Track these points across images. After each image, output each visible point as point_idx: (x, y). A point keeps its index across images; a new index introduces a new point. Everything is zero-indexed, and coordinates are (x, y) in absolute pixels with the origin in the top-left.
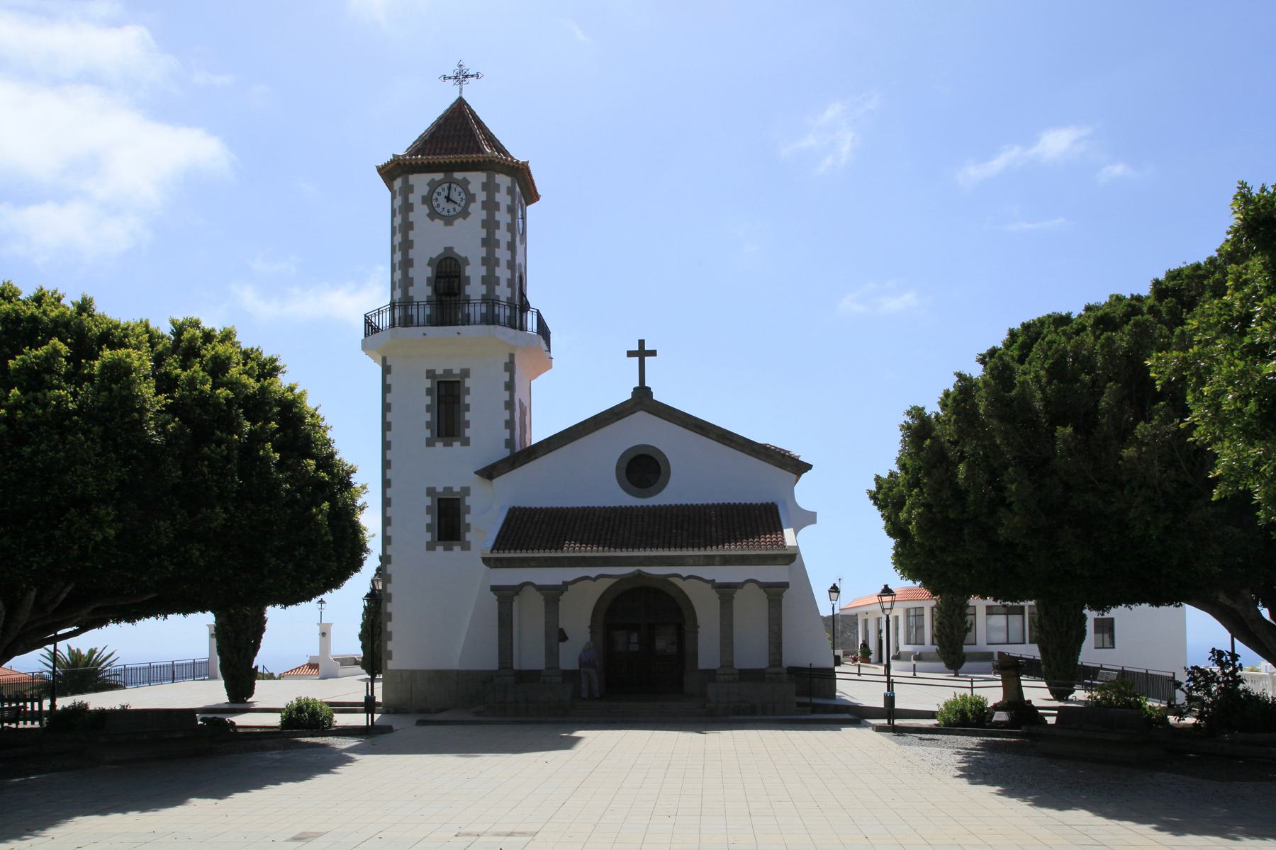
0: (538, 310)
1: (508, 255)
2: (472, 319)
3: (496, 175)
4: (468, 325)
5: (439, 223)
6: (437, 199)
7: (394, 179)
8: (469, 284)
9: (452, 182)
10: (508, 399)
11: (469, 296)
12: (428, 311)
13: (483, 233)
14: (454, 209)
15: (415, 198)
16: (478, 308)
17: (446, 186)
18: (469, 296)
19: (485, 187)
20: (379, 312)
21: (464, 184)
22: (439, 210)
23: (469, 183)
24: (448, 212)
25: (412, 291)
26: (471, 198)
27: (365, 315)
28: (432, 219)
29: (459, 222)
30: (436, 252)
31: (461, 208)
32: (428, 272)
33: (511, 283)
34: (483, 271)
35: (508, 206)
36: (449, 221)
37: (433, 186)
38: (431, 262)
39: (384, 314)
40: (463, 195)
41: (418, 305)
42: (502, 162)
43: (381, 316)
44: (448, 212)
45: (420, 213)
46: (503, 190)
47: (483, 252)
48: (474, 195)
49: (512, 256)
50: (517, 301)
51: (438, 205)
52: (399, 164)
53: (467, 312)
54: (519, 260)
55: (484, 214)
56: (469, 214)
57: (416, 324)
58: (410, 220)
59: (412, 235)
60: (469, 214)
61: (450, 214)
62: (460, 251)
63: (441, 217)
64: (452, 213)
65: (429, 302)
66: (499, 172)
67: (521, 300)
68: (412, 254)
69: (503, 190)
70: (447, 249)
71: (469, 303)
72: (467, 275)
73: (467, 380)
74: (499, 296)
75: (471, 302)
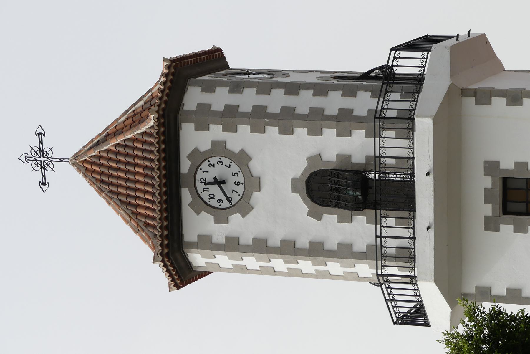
0: (392, 49)
1: (307, 95)
2: (405, 153)
3: (185, 108)
4: (414, 158)
6: (219, 201)
7: (188, 265)
11: (368, 158)
12: (392, 222)
13: (273, 131)
14: (234, 175)
16: (389, 143)
17: (200, 187)
18: (368, 158)
19: (202, 127)
20: (393, 300)
23: (196, 150)
24: (238, 184)
25: (361, 246)
27: (395, 323)
29: (256, 167)
31: (233, 165)
33: (350, 92)
34: (330, 133)
39: (395, 292)
40: (214, 160)
41: (381, 237)
42: (165, 98)
43: (397, 297)
44: (238, 184)
46: (206, 98)
47: (301, 132)
48: (214, 143)
49: (308, 88)
52: (167, 255)
53: (393, 161)
54: (312, 79)
55: (244, 129)
56: (242, 151)
57: (411, 241)
58: (250, 242)
59: (275, 241)
60: (242, 151)
61: (242, 181)
63: (246, 196)
64: (240, 178)
65: (377, 221)
67: (267, 74)
69: (206, 98)
70: (294, 191)
71: (380, 157)
72: (335, 159)
73: (503, 166)
74: (369, 110)
75: (377, 154)
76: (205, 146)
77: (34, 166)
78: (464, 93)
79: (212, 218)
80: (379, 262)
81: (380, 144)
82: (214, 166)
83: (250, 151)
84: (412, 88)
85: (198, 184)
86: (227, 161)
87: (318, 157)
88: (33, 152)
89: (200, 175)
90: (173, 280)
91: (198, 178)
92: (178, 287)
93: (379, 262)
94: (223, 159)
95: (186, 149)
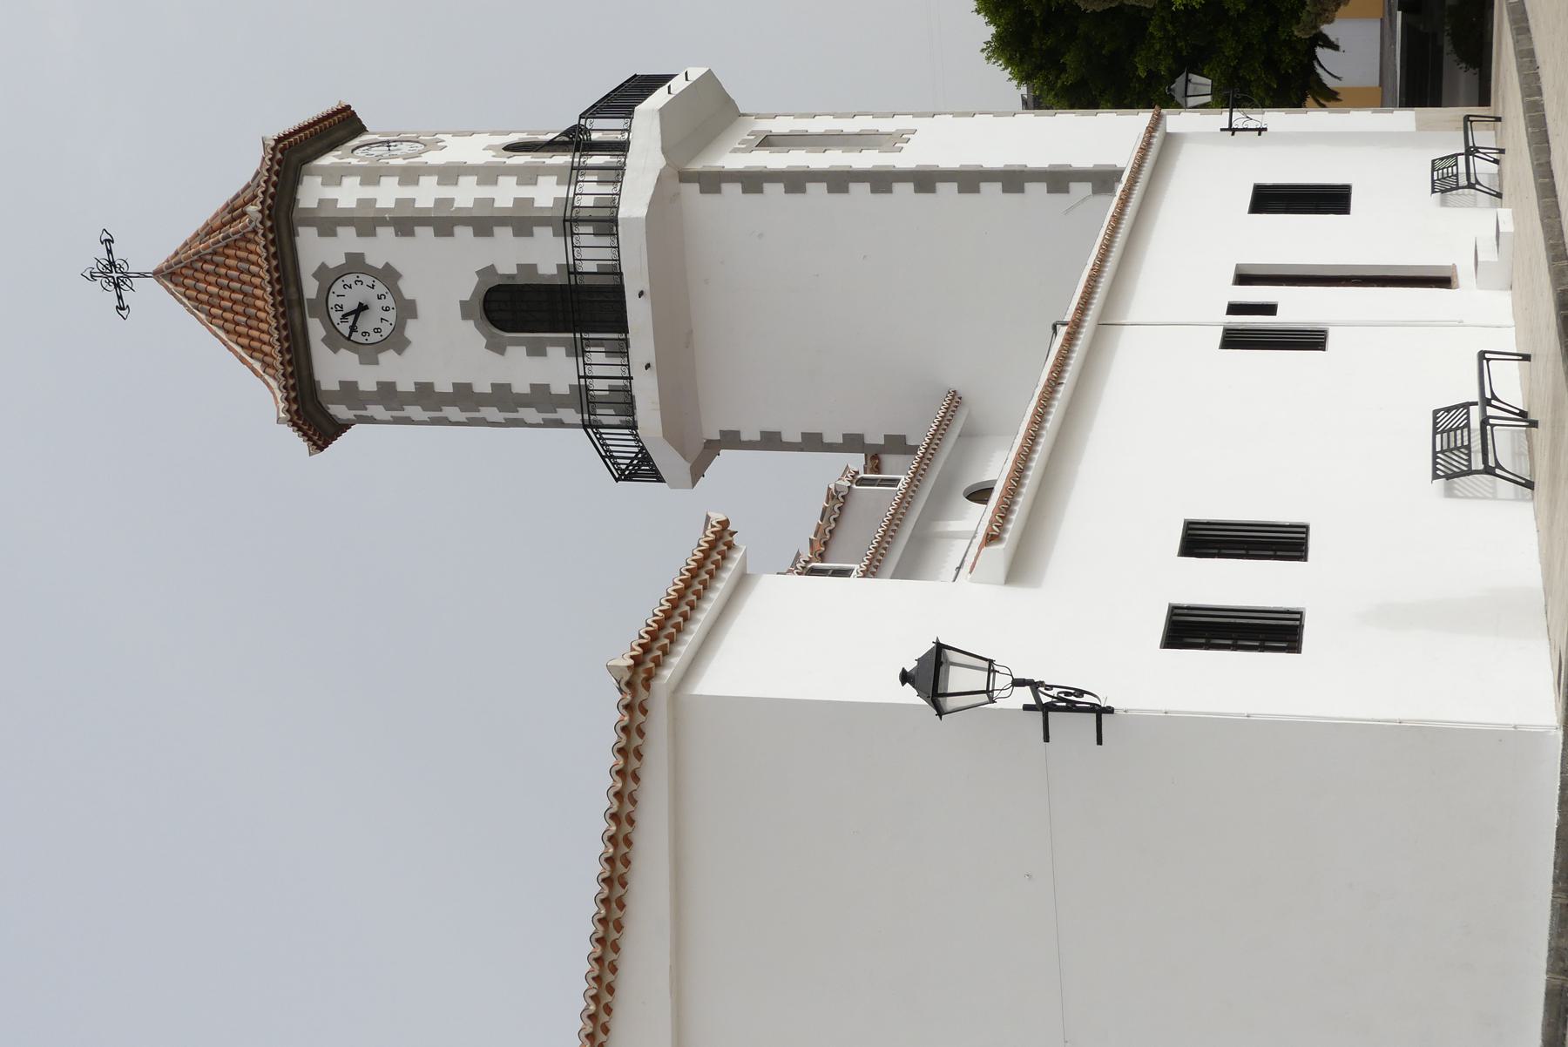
5: (412, 329)
7: (331, 419)
8: (534, 266)
9: (322, 307)
10: (780, 187)
11: (559, 266)
14: (379, 298)
15: (367, 379)
17: (336, 317)
21: (328, 277)
22: (386, 329)
23: (323, 267)
26: (355, 263)
28: (407, 343)
29: (408, 289)
30: (471, 336)
32: (517, 353)
33: (528, 176)
35: (362, 183)
36: (407, 310)
37: (335, 341)
38: (497, 347)
40: (350, 279)
41: (585, 377)
45: (399, 370)
46: (330, 193)
50: (562, 159)
51: (377, 330)
55: (386, 233)
57: (626, 382)
62: (467, 287)
63: (399, 327)
64: (389, 301)
66: (293, 200)
68: (483, 386)
69: (330, 193)
70: (466, 315)
76: (336, 260)
77: (105, 285)
78: (686, 177)
79: (356, 357)
80: (580, 359)
81: (574, 256)
82: (350, 288)
83: (398, 266)
84: (612, 175)
85: (333, 313)
86: (368, 280)
87: (490, 271)
88: (100, 266)
89: (333, 301)
90: (315, 444)
91: (331, 304)
92: (321, 449)
93: (580, 359)
94: (362, 277)
95: (308, 266)
